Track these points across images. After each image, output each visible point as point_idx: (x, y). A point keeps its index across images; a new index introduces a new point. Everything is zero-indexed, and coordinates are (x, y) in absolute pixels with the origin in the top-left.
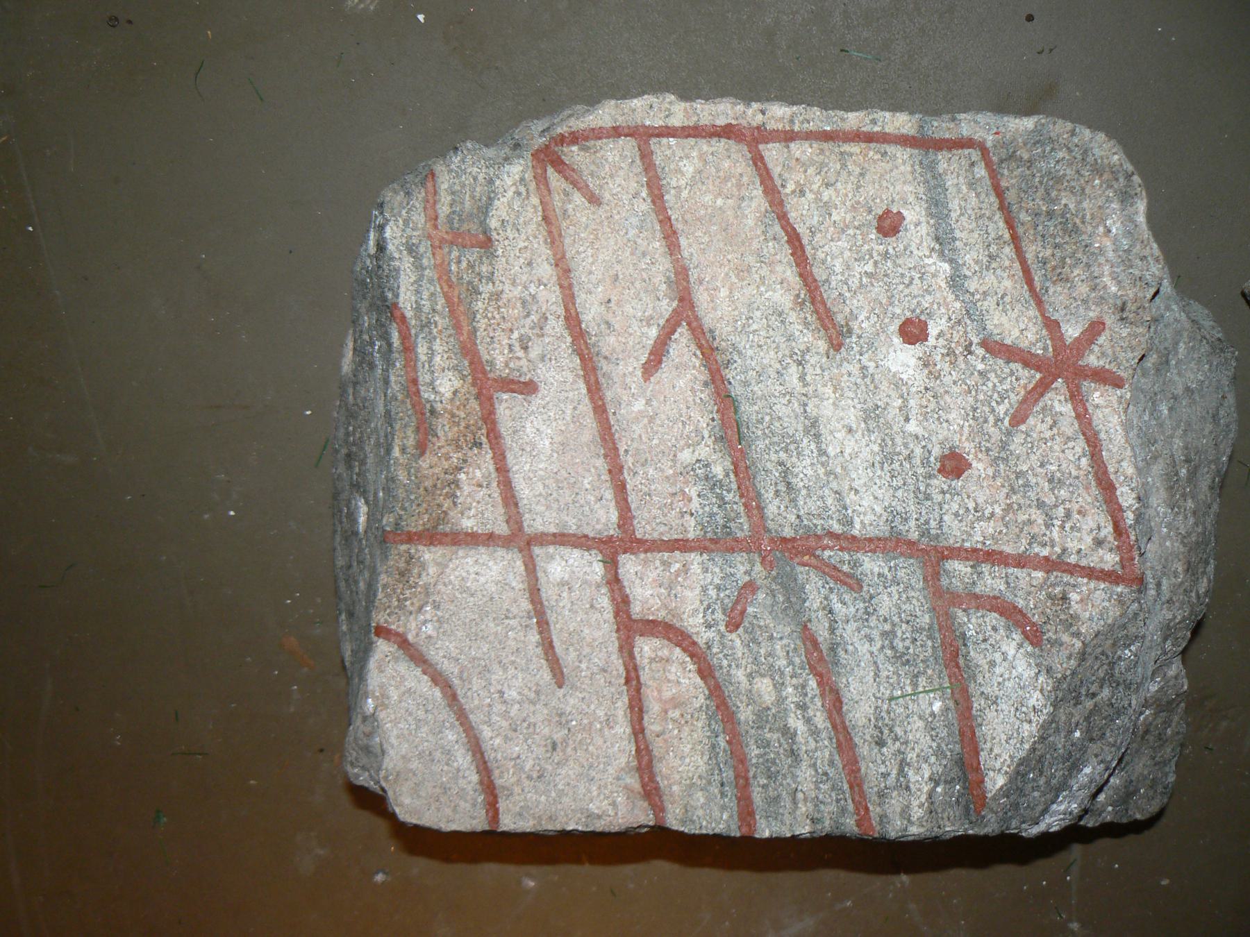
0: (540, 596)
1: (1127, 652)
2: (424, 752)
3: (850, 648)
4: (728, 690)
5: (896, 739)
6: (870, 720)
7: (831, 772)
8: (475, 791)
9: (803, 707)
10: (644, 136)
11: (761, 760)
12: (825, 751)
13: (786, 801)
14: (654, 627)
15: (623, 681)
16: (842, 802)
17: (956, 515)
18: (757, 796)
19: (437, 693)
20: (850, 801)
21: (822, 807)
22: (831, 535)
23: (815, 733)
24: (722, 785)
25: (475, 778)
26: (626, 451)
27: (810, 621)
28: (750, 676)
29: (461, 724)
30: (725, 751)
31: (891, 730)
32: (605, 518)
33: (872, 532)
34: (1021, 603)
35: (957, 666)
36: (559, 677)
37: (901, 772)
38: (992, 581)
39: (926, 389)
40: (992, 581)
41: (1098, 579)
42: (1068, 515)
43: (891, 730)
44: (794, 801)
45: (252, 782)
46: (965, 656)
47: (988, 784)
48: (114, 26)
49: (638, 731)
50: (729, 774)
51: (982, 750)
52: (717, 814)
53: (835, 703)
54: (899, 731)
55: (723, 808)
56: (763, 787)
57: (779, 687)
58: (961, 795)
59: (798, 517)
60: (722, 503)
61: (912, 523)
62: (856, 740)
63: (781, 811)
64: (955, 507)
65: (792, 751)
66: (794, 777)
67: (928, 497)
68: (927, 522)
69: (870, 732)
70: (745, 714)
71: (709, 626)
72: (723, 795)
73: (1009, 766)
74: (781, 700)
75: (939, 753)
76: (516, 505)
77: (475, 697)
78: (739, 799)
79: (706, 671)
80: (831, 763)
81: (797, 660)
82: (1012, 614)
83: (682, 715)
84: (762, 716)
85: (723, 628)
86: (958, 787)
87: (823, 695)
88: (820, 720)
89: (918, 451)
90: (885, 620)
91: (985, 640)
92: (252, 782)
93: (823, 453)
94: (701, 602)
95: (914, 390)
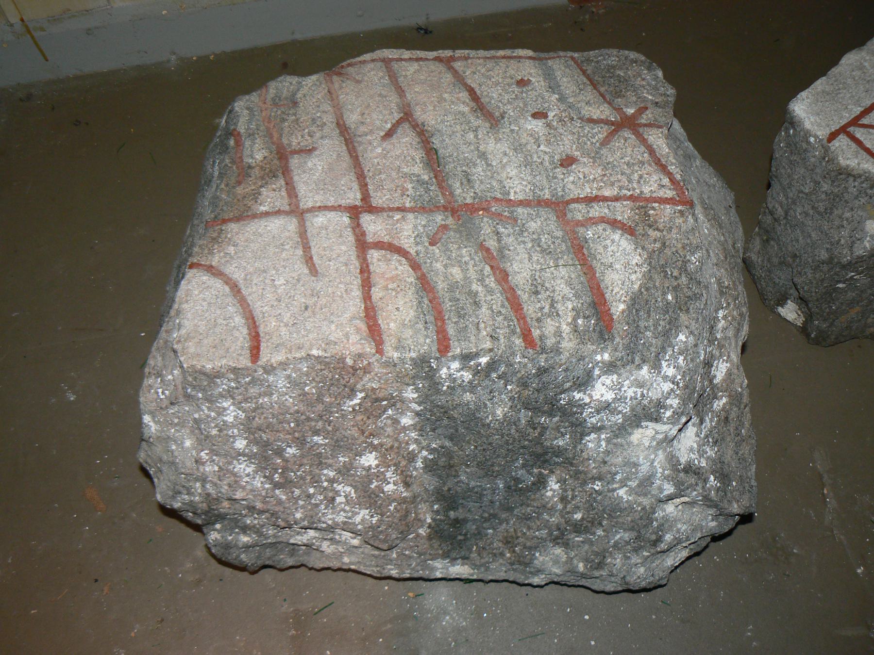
0: (306, 235)
1: (693, 258)
2: (210, 320)
3: (512, 248)
4: (431, 276)
5: (547, 289)
6: (528, 281)
7: (503, 311)
8: (245, 338)
9: (481, 280)
10: (387, 62)
11: (453, 308)
12: (498, 299)
13: (472, 328)
14: (379, 245)
15: (358, 271)
16: (512, 327)
17: (573, 182)
18: (451, 331)
19: (227, 289)
20: (517, 327)
21: (498, 330)
22: (496, 199)
23: (490, 292)
24: (426, 323)
25: (245, 331)
26: (369, 171)
27: (485, 240)
28: (446, 266)
29: (241, 305)
30: (427, 305)
31: (543, 286)
32: (354, 197)
33: (521, 197)
34: (619, 218)
35: (584, 254)
36: (313, 271)
37: (552, 306)
38: (597, 211)
39: (549, 134)
40: (597, 211)
41: (664, 202)
42: (641, 177)
43: (543, 286)
44: (478, 329)
45: (33, 612)
46: (588, 249)
47: (613, 310)
48: (76, 125)
49: (367, 297)
50: (430, 318)
51: (606, 293)
52: (421, 340)
53: (503, 277)
54: (547, 285)
55: (427, 336)
56: (455, 323)
57: (465, 271)
58: (596, 325)
59: (475, 193)
60: (427, 190)
61: (547, 191)
62: (519, 292)
63: (469, 335)
64: (571, 179)
65: (475, 302)
66: (477, 317)
67: (556, 178)
68: (555, 189)
69: (527, 288)
70: (441, 286)
71: (417, 244)
72: (426, 328)
73: (626, 297)
74: (466, 278)
75: (577, 296)
76: (297, 197)
77: (251, 293)
78: (438, 332)
79: (415, 266)
80: (503, 306)
81: (477, 259)
82: (614, 224)
83: (399, 286)
84: (453, 287)
85: (427, 244)
86: (593, 322)
87: (494, 274)
88: (491, 282)
89: (547, 158)
90: (533, 233)
91: (599, 237)
92: (33, 612)
93: (488, 165)
94: (413, 232)
95: (540, 134)
